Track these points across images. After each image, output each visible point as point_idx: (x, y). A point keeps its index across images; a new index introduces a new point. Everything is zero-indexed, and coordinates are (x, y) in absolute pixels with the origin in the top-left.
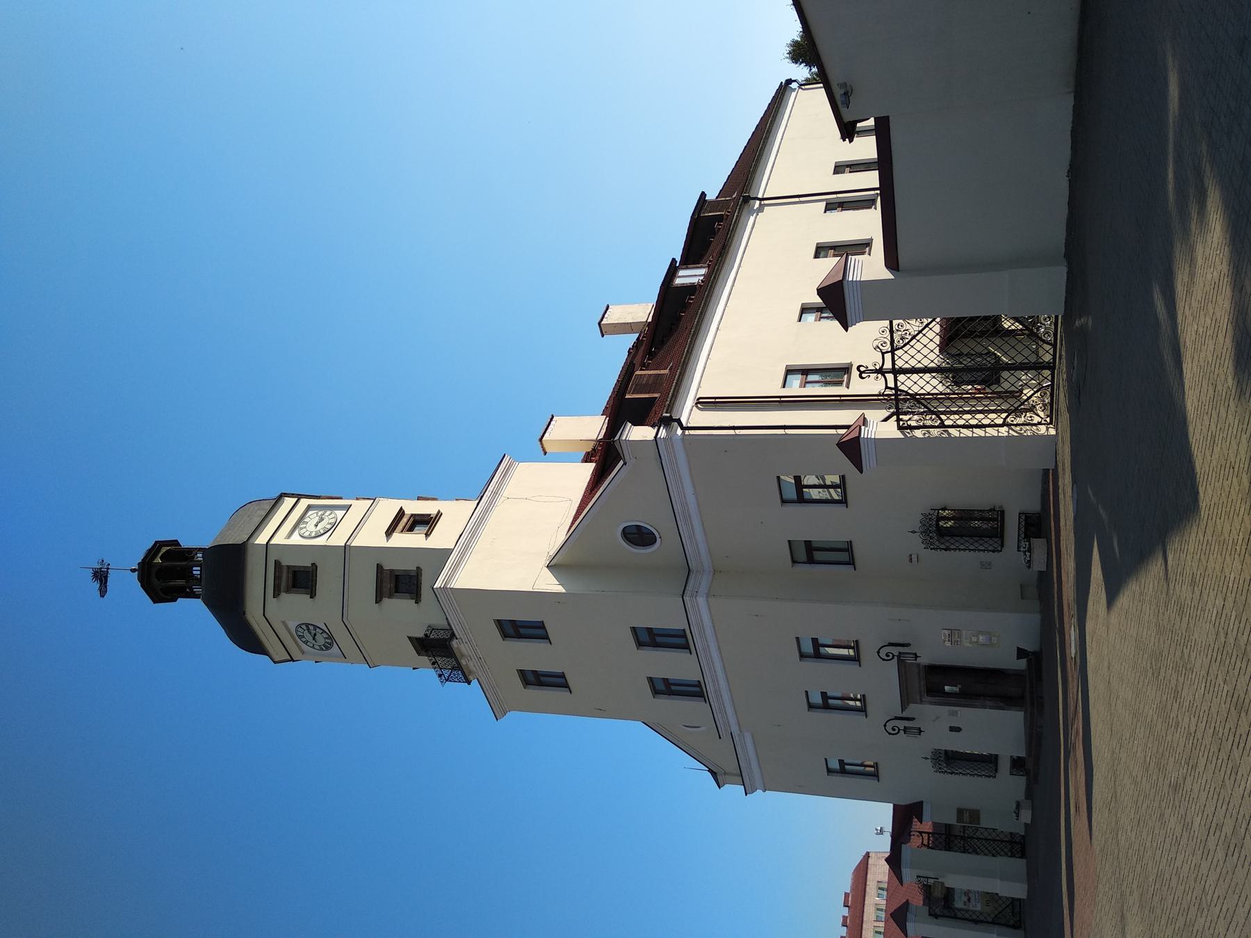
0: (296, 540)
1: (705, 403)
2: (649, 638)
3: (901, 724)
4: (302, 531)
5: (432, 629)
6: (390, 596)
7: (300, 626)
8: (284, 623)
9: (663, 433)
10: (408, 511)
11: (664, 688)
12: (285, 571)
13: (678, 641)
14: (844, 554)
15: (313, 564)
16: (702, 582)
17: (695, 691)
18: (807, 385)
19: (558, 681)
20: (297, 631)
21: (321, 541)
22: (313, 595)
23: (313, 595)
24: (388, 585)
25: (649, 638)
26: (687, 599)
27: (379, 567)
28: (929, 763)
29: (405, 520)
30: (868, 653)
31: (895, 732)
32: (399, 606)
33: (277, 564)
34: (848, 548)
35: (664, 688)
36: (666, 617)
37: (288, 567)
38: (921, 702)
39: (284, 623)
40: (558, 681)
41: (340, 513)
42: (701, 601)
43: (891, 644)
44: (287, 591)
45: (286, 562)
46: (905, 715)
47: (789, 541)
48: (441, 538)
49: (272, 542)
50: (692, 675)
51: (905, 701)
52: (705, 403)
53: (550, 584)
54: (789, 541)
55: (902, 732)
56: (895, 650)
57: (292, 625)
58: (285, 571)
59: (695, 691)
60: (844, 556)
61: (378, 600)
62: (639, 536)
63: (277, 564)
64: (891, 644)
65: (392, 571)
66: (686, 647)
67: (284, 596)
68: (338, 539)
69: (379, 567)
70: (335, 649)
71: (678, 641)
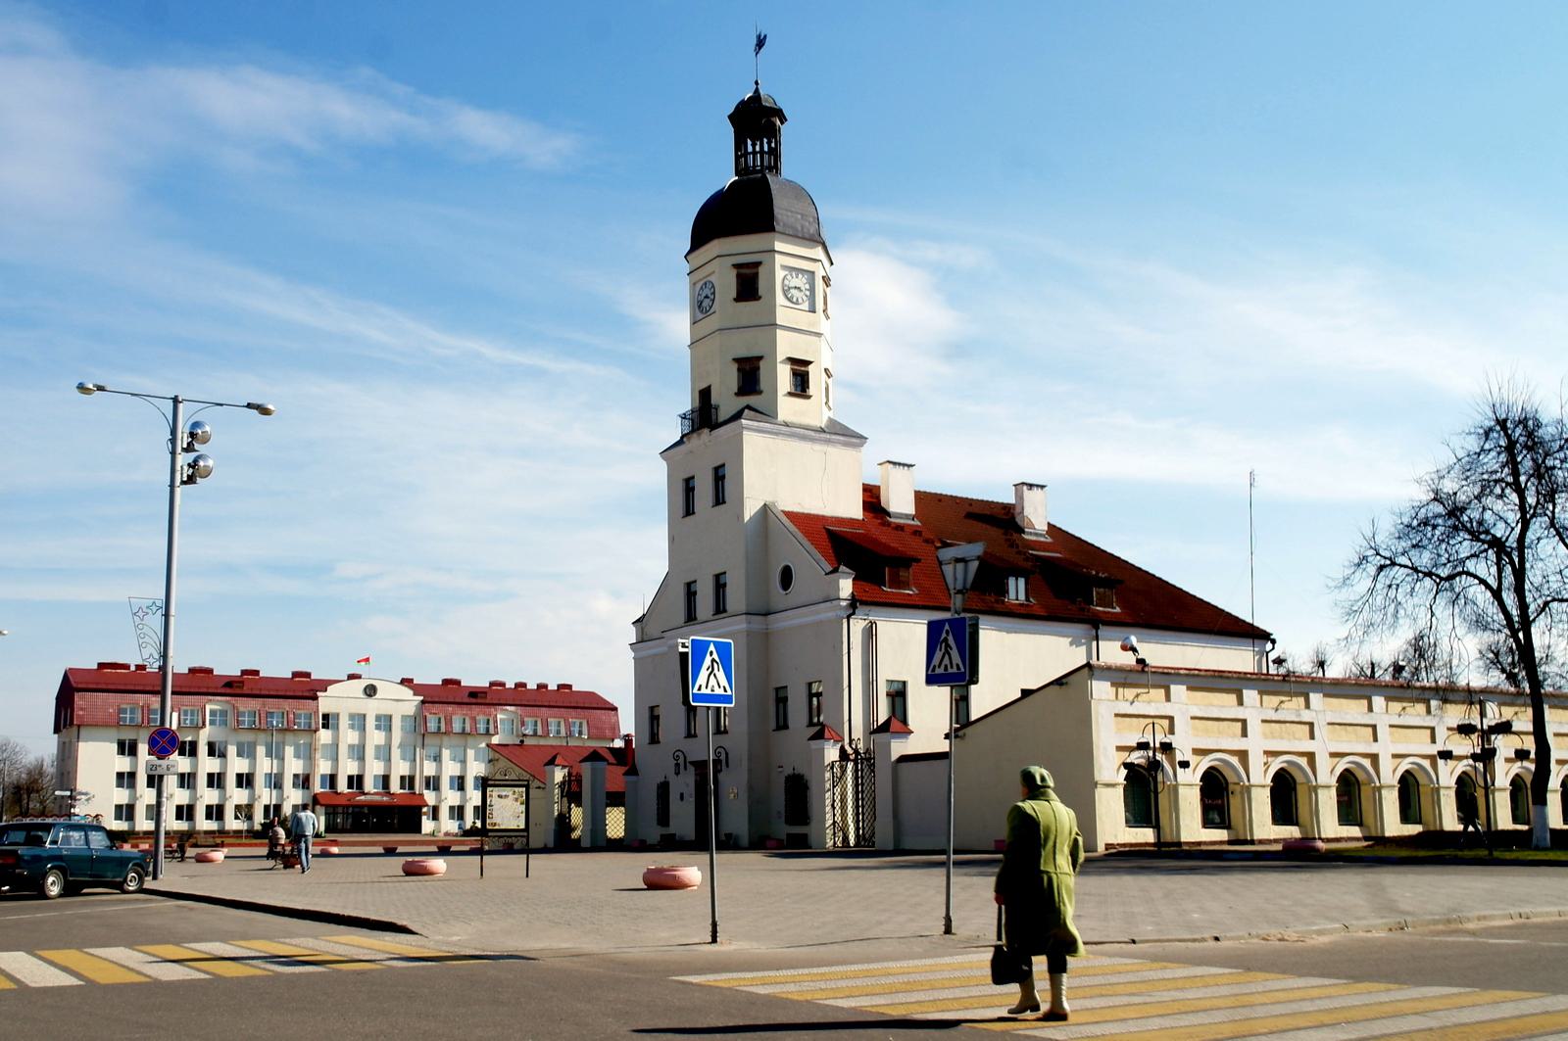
0: (780, 274)
2: (720, 585)
3: (681, 761)
4: (789, 277)
5: (717, 408)
6: (739, 370)
7: (713, 286)
8: (714, 272)
9: (844, 603)
10: (811, 368)
11: (691, 594)
12: (754, 271)
13: (720, 608)
14: (782, 725)
15: (760, 298)
16: (758, 622)
17: (691, 617)
18: (890, 698)
19: (689, 511)
20: (710, 282)
21: (780, 299)
25: (720, 585)
26: (744, 616)
27: (760, 358)
28: (663, 779)
30: (723, 740)
31: (676, 758)
32: (732, 378)
33: (758, 264)
34: (786, 727)
35: (691, 594)
36: (735, 599)
37: (757, 273)
38: (696, 774)
39: (714, 272)
40: (689, 511)
41: (806, 306)
43: (727, 754)
44: (739, 276)
45: (762, 270)
46: (688, 764)
47: (786, 687)
48: (788, 408)
49: (777, 256)
53: (750, 509)
54: (786, 687)
56: (723, 757)
57: (712, 278)
58: (754, 271)
59: (691, 617)
60: (781, 723)
61: (736, 360)
62: (787, 577)
63: (758, 264)
64: (727, 754)
65: (758, 368)
67: (734, 273)
68: (783, 315)
69: (760, 358)
70: (701, 316)
71: (720, 608)
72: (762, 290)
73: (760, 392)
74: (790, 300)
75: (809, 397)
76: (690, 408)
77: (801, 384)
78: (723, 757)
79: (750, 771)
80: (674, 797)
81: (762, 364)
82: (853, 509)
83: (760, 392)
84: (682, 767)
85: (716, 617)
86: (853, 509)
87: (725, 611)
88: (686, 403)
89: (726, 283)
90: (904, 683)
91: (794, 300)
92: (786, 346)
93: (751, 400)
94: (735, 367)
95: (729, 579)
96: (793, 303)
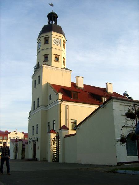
0: (53, 39)
1: (67, 106)
13: (38, 106)
15: (49, 43)
16: (44, 109)
21: (53, 43)
22: (44, 44)
24: (46, 56)
27: (48, 54)
29: (58, 56)
33: (49, 37)
41: (59, 45)
42: (41, 109)
48: (54, 63)
50: (35, 109)
51: (34, 141)
52: (67, 106)
56: (37, 139)
61: (44, 55)
63: (49, 37)
68: (53, 46)
72: (49, 42)
75: (59, 62)
77: (57, 59)
79: (41, 143)
81: (49, 56)
82: (70, 86)
86: (70, 86)
89: (43, 41)
90: (76, 120)
92: (54, 51)
94: (43, 56)
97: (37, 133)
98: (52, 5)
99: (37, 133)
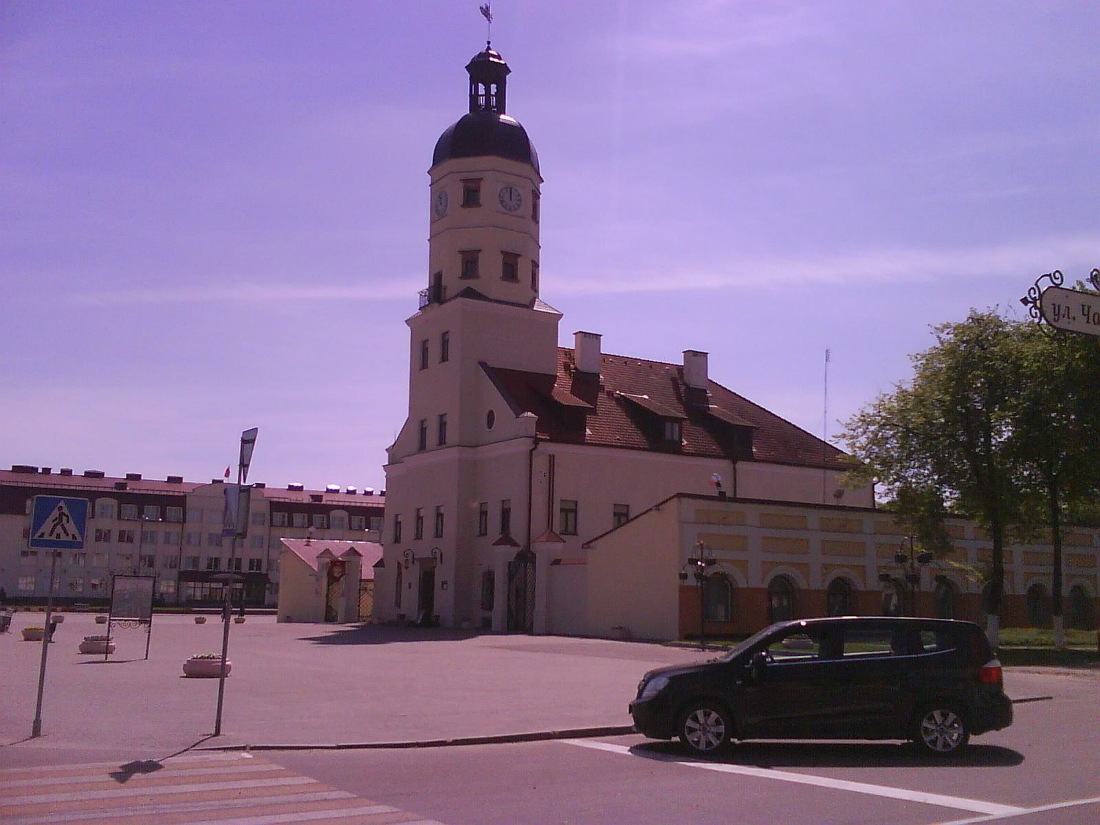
1: (552, 458)
2: (442, 426)
3: (410, 558)
11: (423, 431)
13: (442, 441)
18: (564, 515)
19: (424, 366)
22: (463, 206)
23: (463, 206)
25: (442, 426)
32: (458, 268)
34: (486, 534)
35: (423, 431)
36: (452, 435)
40: (424, 366)
51: (422, 560)
52: (552, 458)
55: (405, 558)
56: (438, 556)
59: (422, 447)
60: (483, 532)
61: (462, 252)
65: (478, 258)
66: (440, 444)
67: (461, 185)
71: (442, 441)
73: (478, 277)
74: (505, 207)
76: (428, 287)
78: (438, 556)
80: (405, 585)
81: (481, 255)
83: (478, 277)
84: (410, 561)
85: (440, 447)
87: (445, 443)
88: (424, 283)
89: (456, 194)
91: (508, 208)
93: (471, 283)
94: (459, 257)
95: (447, 419)
96: (507, 209)
97: (439, 534)
98: (486, 12)
99: (439, 534)
